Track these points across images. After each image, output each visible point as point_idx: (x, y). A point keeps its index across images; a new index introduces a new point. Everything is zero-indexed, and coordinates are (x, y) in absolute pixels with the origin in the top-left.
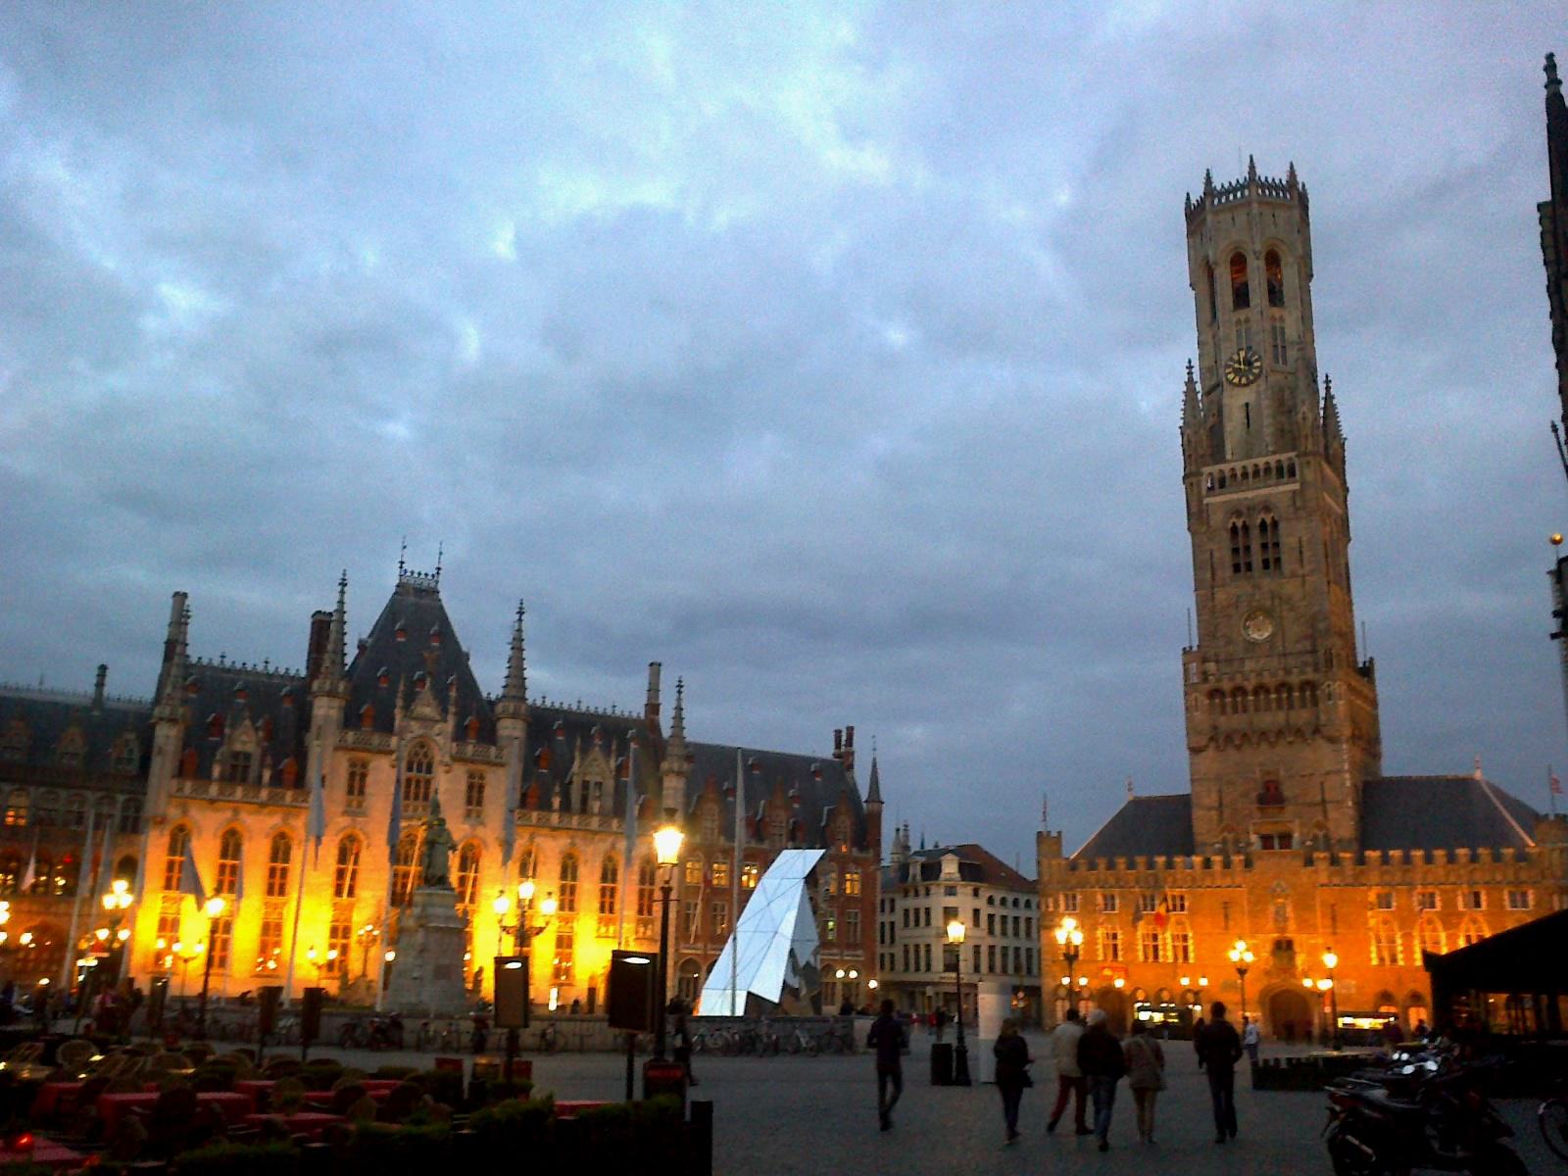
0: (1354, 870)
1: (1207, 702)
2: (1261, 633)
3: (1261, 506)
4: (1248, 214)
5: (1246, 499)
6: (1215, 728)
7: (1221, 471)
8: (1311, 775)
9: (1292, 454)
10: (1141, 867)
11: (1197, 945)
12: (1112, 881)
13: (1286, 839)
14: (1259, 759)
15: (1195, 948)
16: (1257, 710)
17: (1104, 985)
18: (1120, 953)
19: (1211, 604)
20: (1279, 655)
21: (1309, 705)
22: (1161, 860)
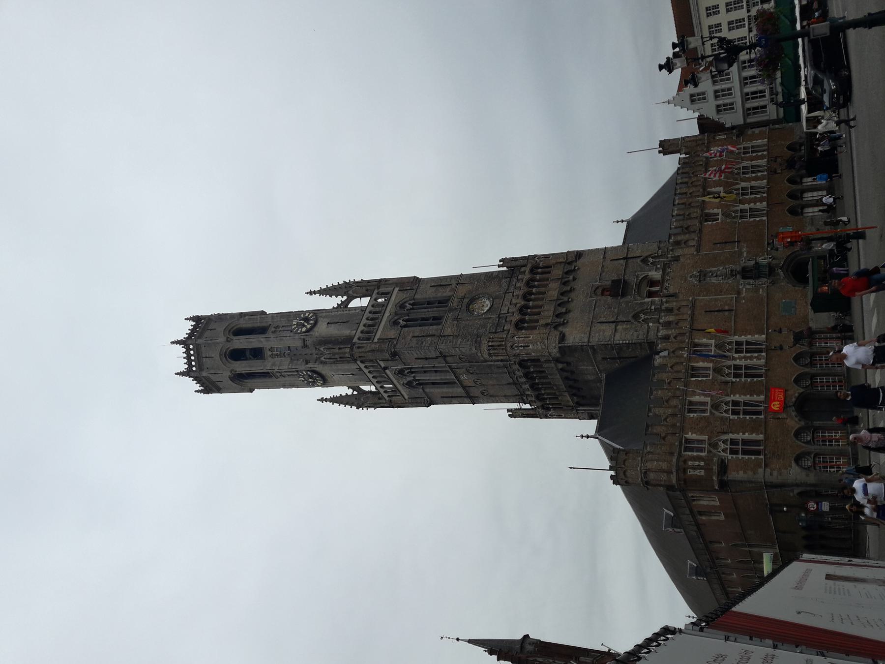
0: (685, 234)
1: (523, 331)
2: (487, 304)
3: (398, 308)
4: (216, 322)
5: (388, 316)
6: (547, 325)
7: (362, 332)
8: (603, 266)
9: (376, 291)
10: (664, 376)
11: (746, 332)
12: (674, 402)
13: (653, 283)
14: (580, 298)
15: (749, 335)
16: (542, 299)
17: (794, 414)
18: (755, 397)
19: (452, 337)
20: (506, 293)
21: (549, 269)
22: (658, 361)
